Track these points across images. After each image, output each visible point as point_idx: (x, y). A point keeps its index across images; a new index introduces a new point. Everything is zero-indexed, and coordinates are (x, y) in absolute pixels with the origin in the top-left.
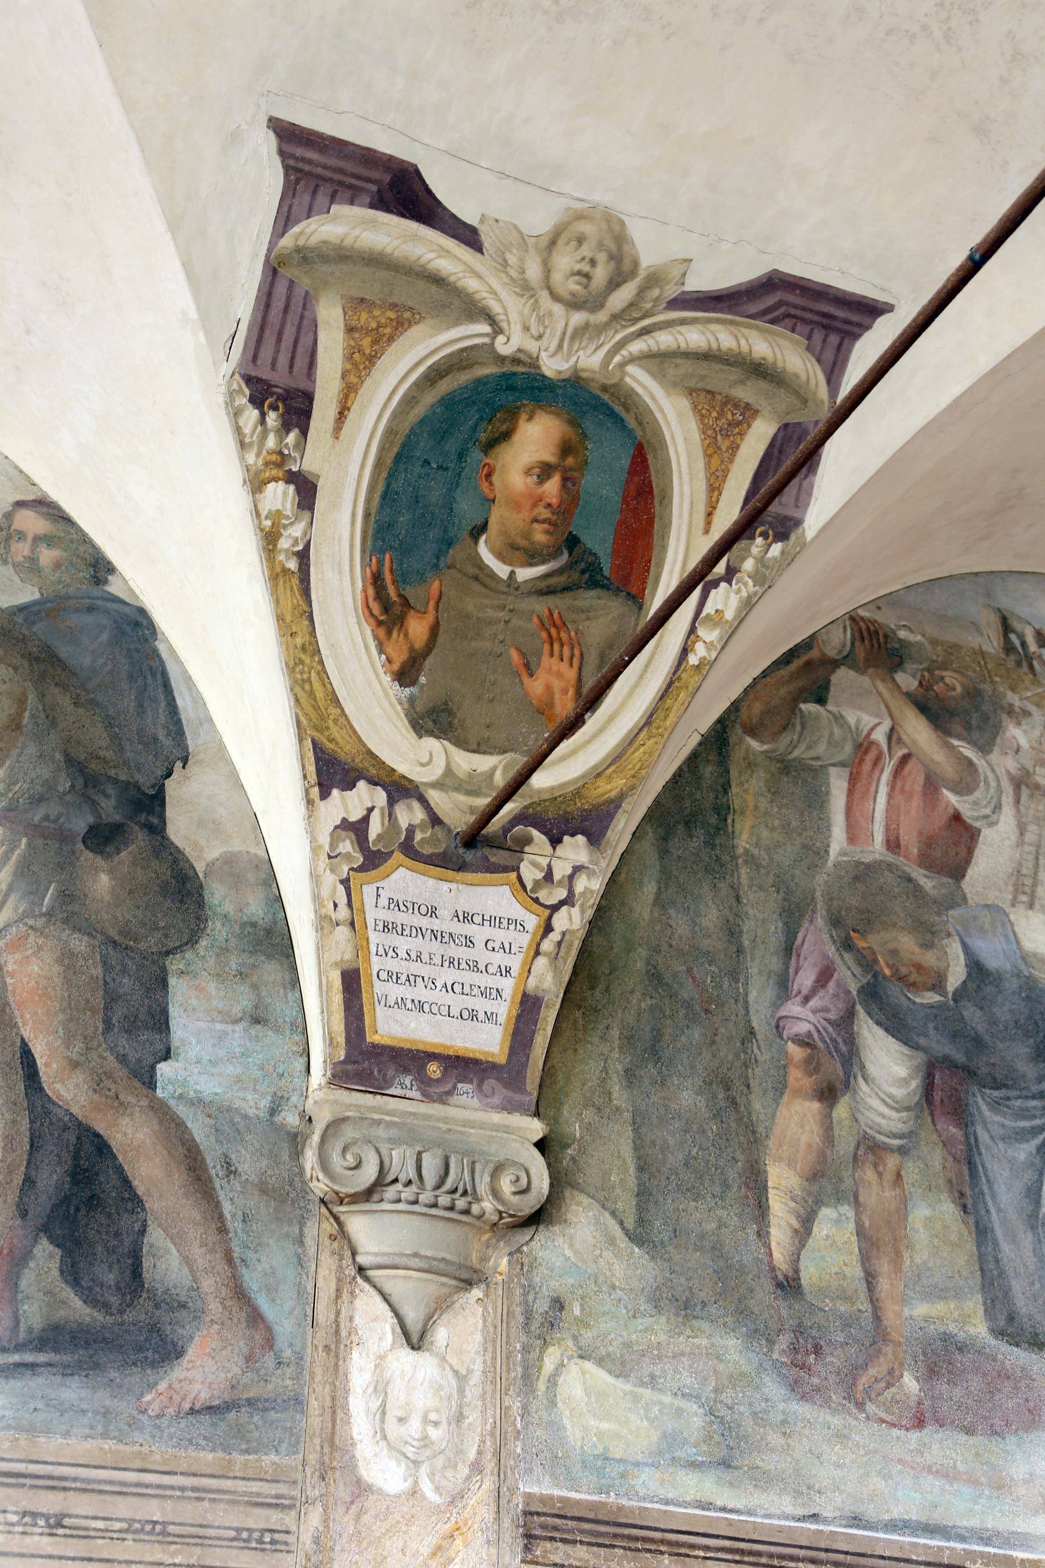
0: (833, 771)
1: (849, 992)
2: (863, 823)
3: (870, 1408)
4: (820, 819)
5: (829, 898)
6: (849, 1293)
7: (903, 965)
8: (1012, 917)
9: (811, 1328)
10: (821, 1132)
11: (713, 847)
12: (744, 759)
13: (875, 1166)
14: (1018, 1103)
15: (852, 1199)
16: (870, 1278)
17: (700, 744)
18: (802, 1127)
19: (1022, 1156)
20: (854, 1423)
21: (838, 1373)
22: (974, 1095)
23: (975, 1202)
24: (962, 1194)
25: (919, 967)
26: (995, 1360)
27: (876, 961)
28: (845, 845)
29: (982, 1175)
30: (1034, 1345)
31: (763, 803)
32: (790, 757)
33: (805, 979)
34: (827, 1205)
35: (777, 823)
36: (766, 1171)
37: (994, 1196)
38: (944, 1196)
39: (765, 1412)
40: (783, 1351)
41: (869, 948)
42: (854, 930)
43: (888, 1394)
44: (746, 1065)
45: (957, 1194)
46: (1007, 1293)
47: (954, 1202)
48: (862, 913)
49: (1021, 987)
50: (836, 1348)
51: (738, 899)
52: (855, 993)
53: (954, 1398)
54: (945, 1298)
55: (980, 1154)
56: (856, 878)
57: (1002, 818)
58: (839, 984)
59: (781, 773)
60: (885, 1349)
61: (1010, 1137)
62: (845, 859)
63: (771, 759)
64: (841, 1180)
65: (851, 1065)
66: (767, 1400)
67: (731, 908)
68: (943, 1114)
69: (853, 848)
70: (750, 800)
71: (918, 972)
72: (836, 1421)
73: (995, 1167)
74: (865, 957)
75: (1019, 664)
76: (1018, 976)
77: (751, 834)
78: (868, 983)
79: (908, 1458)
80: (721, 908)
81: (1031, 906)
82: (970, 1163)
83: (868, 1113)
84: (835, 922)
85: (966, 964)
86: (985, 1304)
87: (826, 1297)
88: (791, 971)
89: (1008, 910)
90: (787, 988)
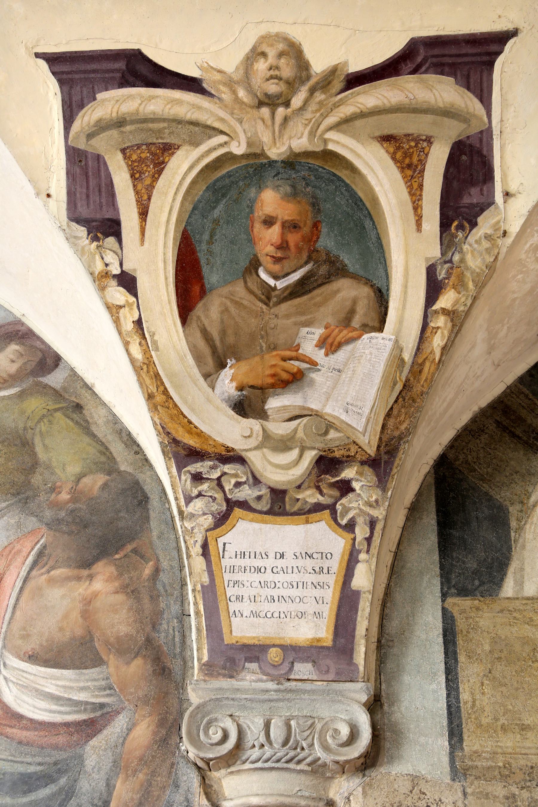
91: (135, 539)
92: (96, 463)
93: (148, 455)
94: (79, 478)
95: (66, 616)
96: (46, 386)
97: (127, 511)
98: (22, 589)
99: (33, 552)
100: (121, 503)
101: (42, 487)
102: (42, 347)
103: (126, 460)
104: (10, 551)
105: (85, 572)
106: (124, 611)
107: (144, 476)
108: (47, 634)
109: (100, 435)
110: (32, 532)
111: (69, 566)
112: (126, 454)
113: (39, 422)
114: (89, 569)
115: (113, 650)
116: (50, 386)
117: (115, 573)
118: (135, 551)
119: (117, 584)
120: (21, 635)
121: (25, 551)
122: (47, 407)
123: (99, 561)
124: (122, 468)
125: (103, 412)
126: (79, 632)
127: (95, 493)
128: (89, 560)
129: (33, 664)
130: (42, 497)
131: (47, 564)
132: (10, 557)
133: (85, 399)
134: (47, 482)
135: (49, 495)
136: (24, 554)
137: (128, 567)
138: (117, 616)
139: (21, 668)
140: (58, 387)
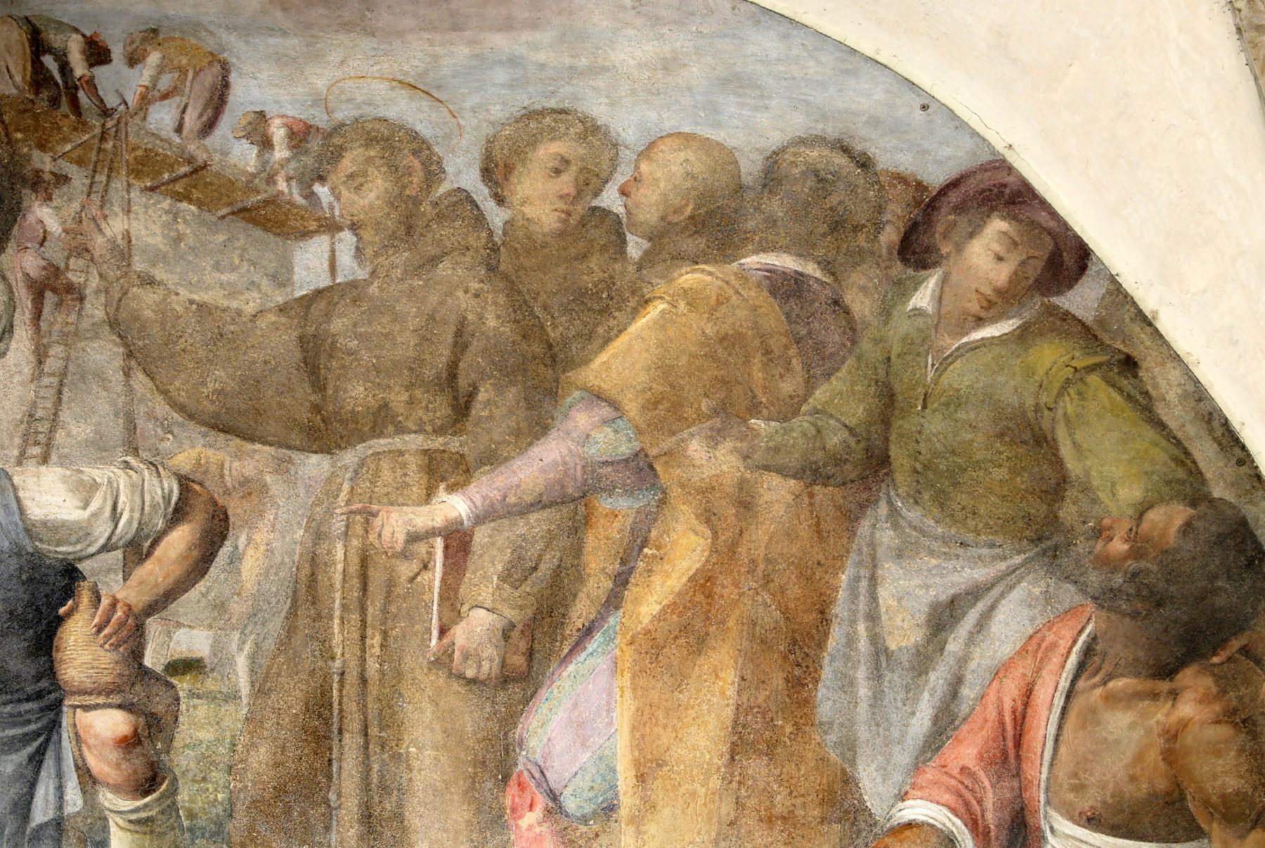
8: (16, 480)
19: (9, 769)
49: (21, 568)
57: (13, 345)
75: (54, 102)
76: (19, 555)
81: (45, 459)
91: (1244, 629)
92: (1168, 483)
93: (1261, 468)
94: (1141, 512)
95: (1139, 758)
96: (1066, 316)
97: (1229, 578)
98: (1064, 711)
99: (1076, 649)
100: (1218, 563)
101: (1080, 528)
102: (1052, 224)
103: (1222, 475)
104: (1039, 645)
105: (1164, 686)
106: (1233, 753)
107: (1255, 509)
108: (1111, 786)
109: (1172, 424)
110: (1070, 612)
111: (1137, 675)
112: (1221, 464)
113: (1060, 395)
114: (1171, 680)
115: (1217, 816)
116: (1074, 316)
117: (1214, 689)
118: (1245, 651)
119: (1217, 708)
120: (1071, 785)
121: (1063, 644)
122: (1074, 363)
123: (1186, 667)
124: (1217, 493)
125: (1175, 375)
126: (1162, 785)
127: (1171, 542)
128: (1168, 664)
129: (1095, 832)
130: (1081, 547)
131: (1100, 669)
132: (1040, 655)
133: (1142, 348)
134: (1086, 517)
135: (1092, 543)
136: (1062, 650)
137: (1235, 679)
138: (1221, 762)
139: (1077, 836)
140: (1088, 316)
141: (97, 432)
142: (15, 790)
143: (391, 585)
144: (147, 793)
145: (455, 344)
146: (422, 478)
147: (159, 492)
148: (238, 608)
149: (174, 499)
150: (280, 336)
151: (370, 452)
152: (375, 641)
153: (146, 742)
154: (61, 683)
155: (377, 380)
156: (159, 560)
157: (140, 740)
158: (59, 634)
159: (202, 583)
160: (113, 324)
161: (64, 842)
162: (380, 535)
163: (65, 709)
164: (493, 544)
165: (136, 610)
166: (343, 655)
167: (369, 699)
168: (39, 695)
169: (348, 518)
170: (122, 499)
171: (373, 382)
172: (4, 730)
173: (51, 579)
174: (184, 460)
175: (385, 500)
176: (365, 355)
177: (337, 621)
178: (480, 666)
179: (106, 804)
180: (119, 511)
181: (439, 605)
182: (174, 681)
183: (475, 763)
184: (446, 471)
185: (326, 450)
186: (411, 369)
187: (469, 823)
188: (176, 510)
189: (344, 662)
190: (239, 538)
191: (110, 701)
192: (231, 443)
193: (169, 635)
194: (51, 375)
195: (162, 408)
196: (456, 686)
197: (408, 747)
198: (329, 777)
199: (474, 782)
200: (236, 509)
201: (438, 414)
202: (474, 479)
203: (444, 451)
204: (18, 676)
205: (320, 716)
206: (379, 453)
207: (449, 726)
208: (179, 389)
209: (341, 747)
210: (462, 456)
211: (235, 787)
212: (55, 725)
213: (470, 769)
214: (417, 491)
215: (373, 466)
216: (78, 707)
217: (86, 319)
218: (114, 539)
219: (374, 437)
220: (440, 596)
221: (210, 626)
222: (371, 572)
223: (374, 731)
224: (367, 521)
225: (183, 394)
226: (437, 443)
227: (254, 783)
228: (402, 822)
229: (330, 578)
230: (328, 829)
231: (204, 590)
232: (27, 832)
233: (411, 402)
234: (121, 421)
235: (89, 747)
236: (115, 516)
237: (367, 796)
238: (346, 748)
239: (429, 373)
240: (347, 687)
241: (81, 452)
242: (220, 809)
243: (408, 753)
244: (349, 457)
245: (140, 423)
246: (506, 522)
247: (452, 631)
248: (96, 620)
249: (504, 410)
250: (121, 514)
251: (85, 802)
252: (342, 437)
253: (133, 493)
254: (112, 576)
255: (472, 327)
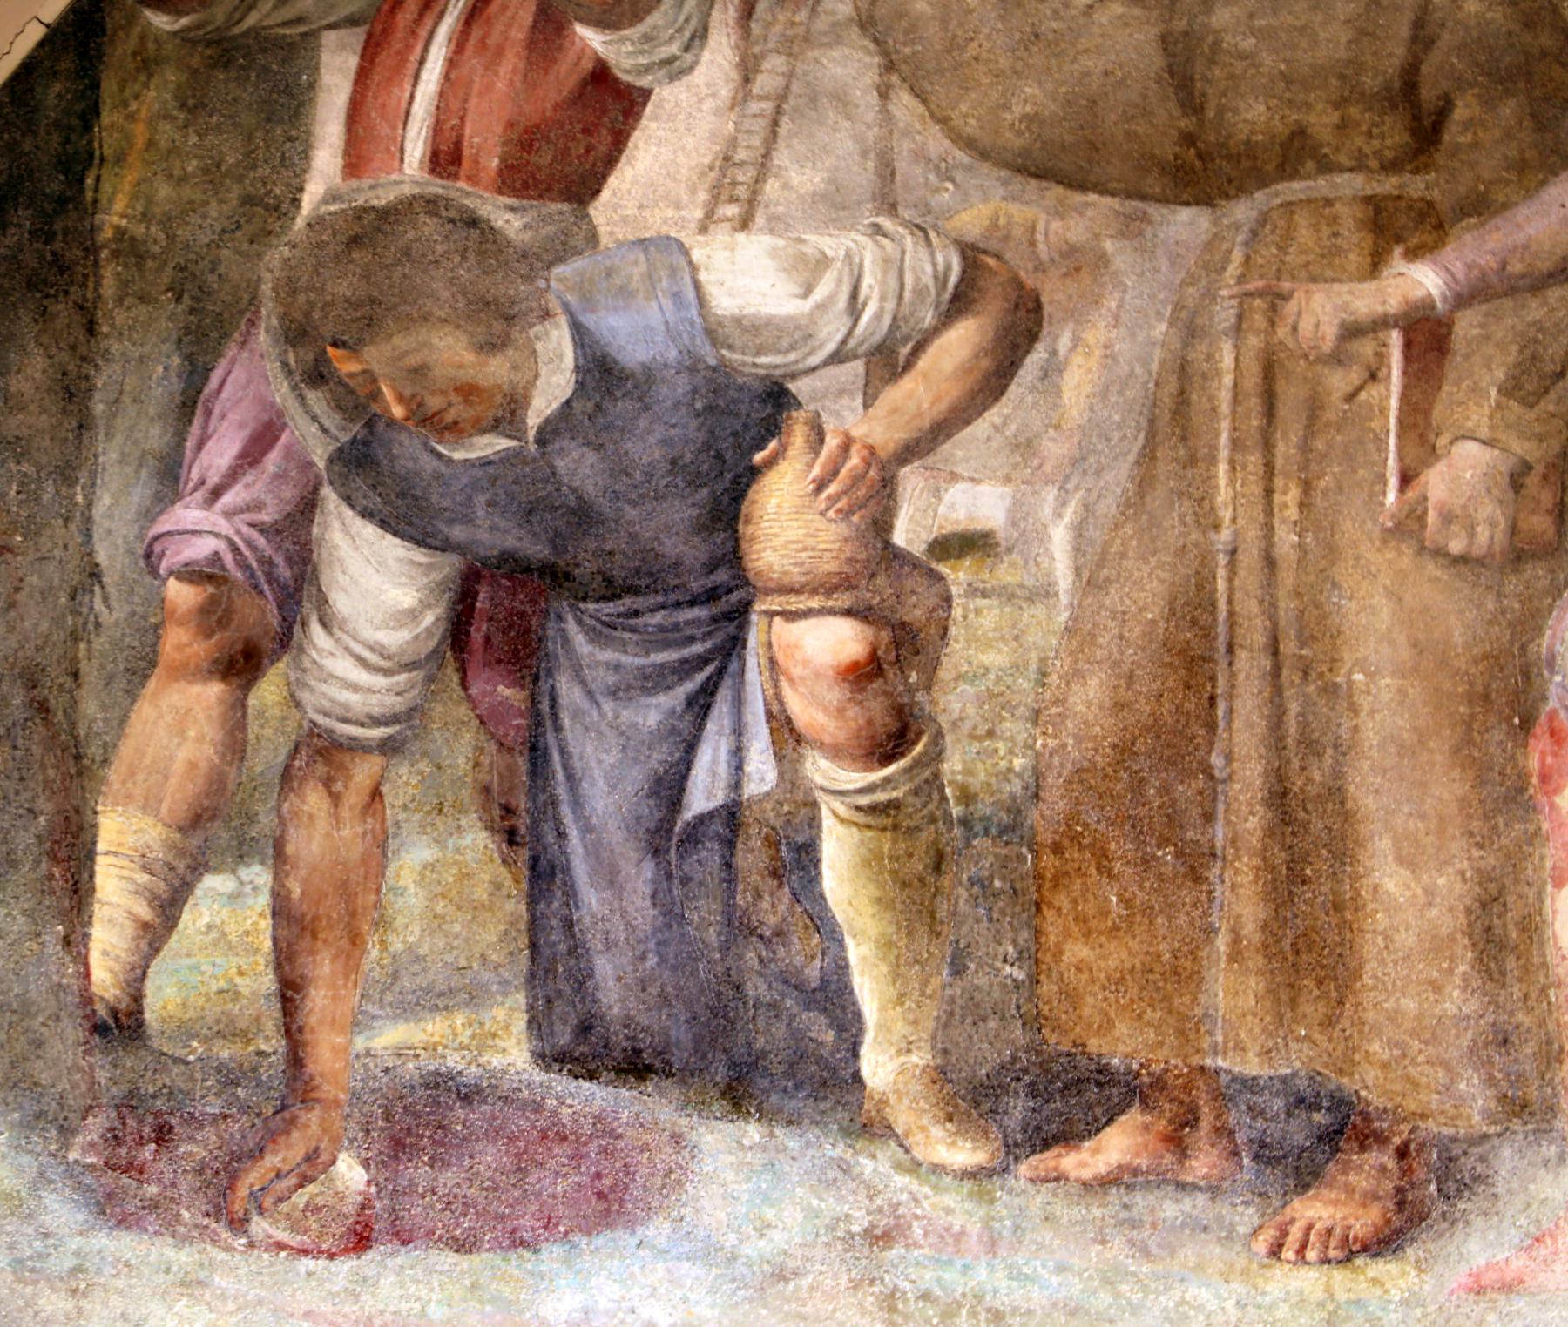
0: (330, 38)
1: (311, 464)
2: (384, 130)
3: (259, 1226)
4: (290, 139)
5: (289, 288)
6: (242, 1024)
7: (433, 393)
8: (696, 255)
9: (154, 1096)
10: (219, 736)
11: (50, 237)
12: (135, 54)
13: (328, 782)
14: (658, 618)
15: (270, 851)
16: (290, 992)
17: (41, 44)
18: (182, 733)
19: (652, 719)
20: (222, 1256)
21: (200, 1172)
22: (560, 618)
23: (535, 826)
24: (508, 811)
25: (468, 392)
26: (538, 1108)
27: (376, 395)
28: (338, 180)
29: (558, 768)
30: (627, 1072)
31: (167, 133)
32: (237, 30)
33: (220, 453)
34: (217, 870)
35: (192, 166)
36: (94, 826)
37: (577, 803)
38: (471, 820)
39: (40, 1256)
40: (92, 1145)
41: (364, 372)
42: (335, 345)
43: (300, 1198)
44: (75, 637)
45: (497, 812)
46: (582, 981)
47: (490, 828)
48: (359, 305)
49: (695, 391)
50: (201, 1127)
51: (91, 328)
52: (321, 464)
53: (441, 1191)
54: (446, 1008)
55: (558, 728)
56: (355, 241)
57: (706, 56)
58: (288, 454)
59: (213, 67)
60: (303, 1117)
61: (629, 687)
62: (333, 208)
63: (194, 42)
64: (251, 819)
65: (299, 603)
66: (46, 1235)
67: (73, 348)
68: (487, 664)
69: (354, 183)
70: (140, 132)
71: (466, 401)
72: (183, 1257)
73: (589, 750)
74: (352, 392)
76: (692, 370)
77: (134, 197)
78: (354, 441)
79: (326, 1308)
80: (54, 351)
81: (745, 223)
82: (533, 748)
83: (324, 687)
84: (295, 333)
85: (577, 368)
86: (531, 1008)
87: (195, 1036)
88: (190, 444)
89: (687, 242)
90: (176, 479)
141: (831, 181)
142: (660, 757)
143: (1314, 407)
144: (887, 759)
145: (1414, 39)
146: (1363, 239)
147: (929, 269)
148: (1054, 449)
149: (953, 279)
150: (1131, 35)
151: (1278, 201)
152: (1288, 497)
153: (891, 672)
154: (750, 575)
155: (1287, 95)
156: (925, 375)
157: (880, 668)
158: (751, 494)
159: (995, 410)
160: (866, 23)
161: (740, 846)
162: (1295, 329)
163: (754, 618)
164: (1488, 338)
165: (883, 455)
166: (1234, 520)
167: (1281, 593)
168: (712, 595)
169: (1241, 304)
170: (867, 281)
171: (1280, 99)
172: (648, 653)
173: (744, 409)
174: (971, 221)
175: (1304, 274)
176: (1267, 59)
177: (1222, 468)
178: (1472, 534)
179: (819, 779)
180: (861, 299)
181: (1399, 437)
182: (943, 569)
183: (1470, 699)
184: (1404, 227)
185: (1205, 200)
186: (1342, 77)
187: (1463, 802)
188: (957, 297)
189: (1236, 533)
190: (1059, 338)
191: (830, 603)
192: (1048, 193)
193: (937, 494)
194: (761, 98)
195: (936, 142)
196: (1432, 569)
197: (1350, 673)
198: (1211, 727)
199: (1470, 729)
200: (1053, 293)
201: (1388, 142)
202: (1451, 238)
203: (1399, 197)
204: (677, 564)
205: (1194, 622)
206: (1290, 204)
207: (1421, 636)
208: (966, 116)
209: (1233, 675)
210: (1430, 204)
211: (1044, 746)
212: (735, 645)
213: (1462, 709)
214: (1355, 259)
215: (1282, 223)
216: (777, 613)
217: (823, 17)
218: (852, 343)
219: (1282, 179)
220: (1400, 422)
221: (1007, 479)
222: (1281, 385)
223: (1289, 647)
224: (1273, 308)
225: (972, 121)
226: (1388, 185)
227: (1078, 739)
228: (1342, 803)
229: (1211, 399)
230: (1208, 817)
231: (998, 420)
232: (677, 829)
233: (1343, 126)
234: (871, 164)
235: (791, 681)
236: (855, 307)
237: (1279, 757)
238: (1241, 677)
239: (1371, 83)
240: (1242, 573)
241: (804, 212)
242: (1016, 786)
243: (1350, 683)
244: (1243, 211)
245: (902, 166)
246: (1508, 303)
247: (1422, 478)
248: (816, 471)
249: (1497, 133)
250: (865, 305)
251: (781, 776)
252: (1230, 181)
253: (885, 272)
254: (845, 401)
255: (1439, 14)
